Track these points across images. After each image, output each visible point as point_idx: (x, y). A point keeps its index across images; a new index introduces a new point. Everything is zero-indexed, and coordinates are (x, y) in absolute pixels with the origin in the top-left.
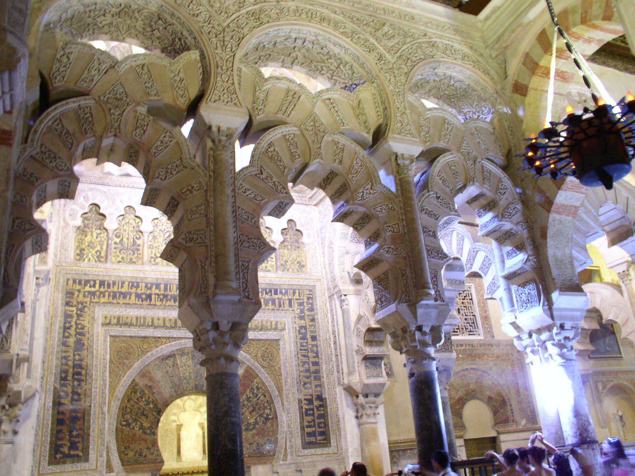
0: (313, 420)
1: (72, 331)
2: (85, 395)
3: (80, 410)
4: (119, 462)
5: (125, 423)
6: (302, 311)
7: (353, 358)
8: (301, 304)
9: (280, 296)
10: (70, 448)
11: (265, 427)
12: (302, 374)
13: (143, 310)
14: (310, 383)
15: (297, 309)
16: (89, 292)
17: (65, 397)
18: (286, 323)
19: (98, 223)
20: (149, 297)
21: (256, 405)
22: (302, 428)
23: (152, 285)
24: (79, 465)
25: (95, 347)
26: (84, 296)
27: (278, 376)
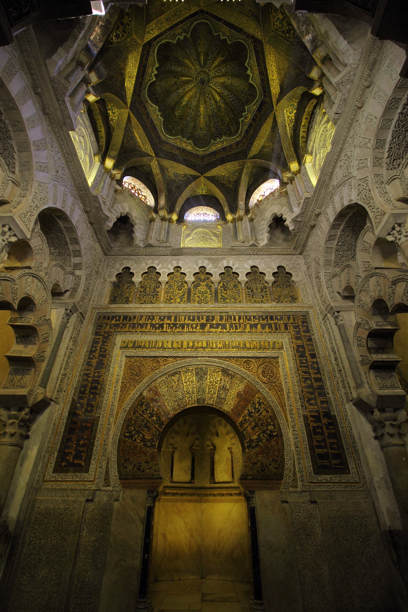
0: (324, 440)
1: (97, 354)
2: (97, 407)
3: (90, 420)
4: (117, 475)
5: (128, 435)
6: (298, 333)
7: (358, 370)
8: (295, 327)
9: (276, 321)
10: (75, 457)
11: (270, 445)
12: (304, 389)
13: (155, 336)
14: (315, 399)
15: (293, 331)
16: (115, 325)
17: (80, 408)
18: (283, 343)
19: (129, 280)
20: (162, 326)
21: (258, 420)
22: (312, 448)
23: (165, 317)
24: (79, 474)
25: (112, 366)
26: (110, 327)
27: (279, 391)
